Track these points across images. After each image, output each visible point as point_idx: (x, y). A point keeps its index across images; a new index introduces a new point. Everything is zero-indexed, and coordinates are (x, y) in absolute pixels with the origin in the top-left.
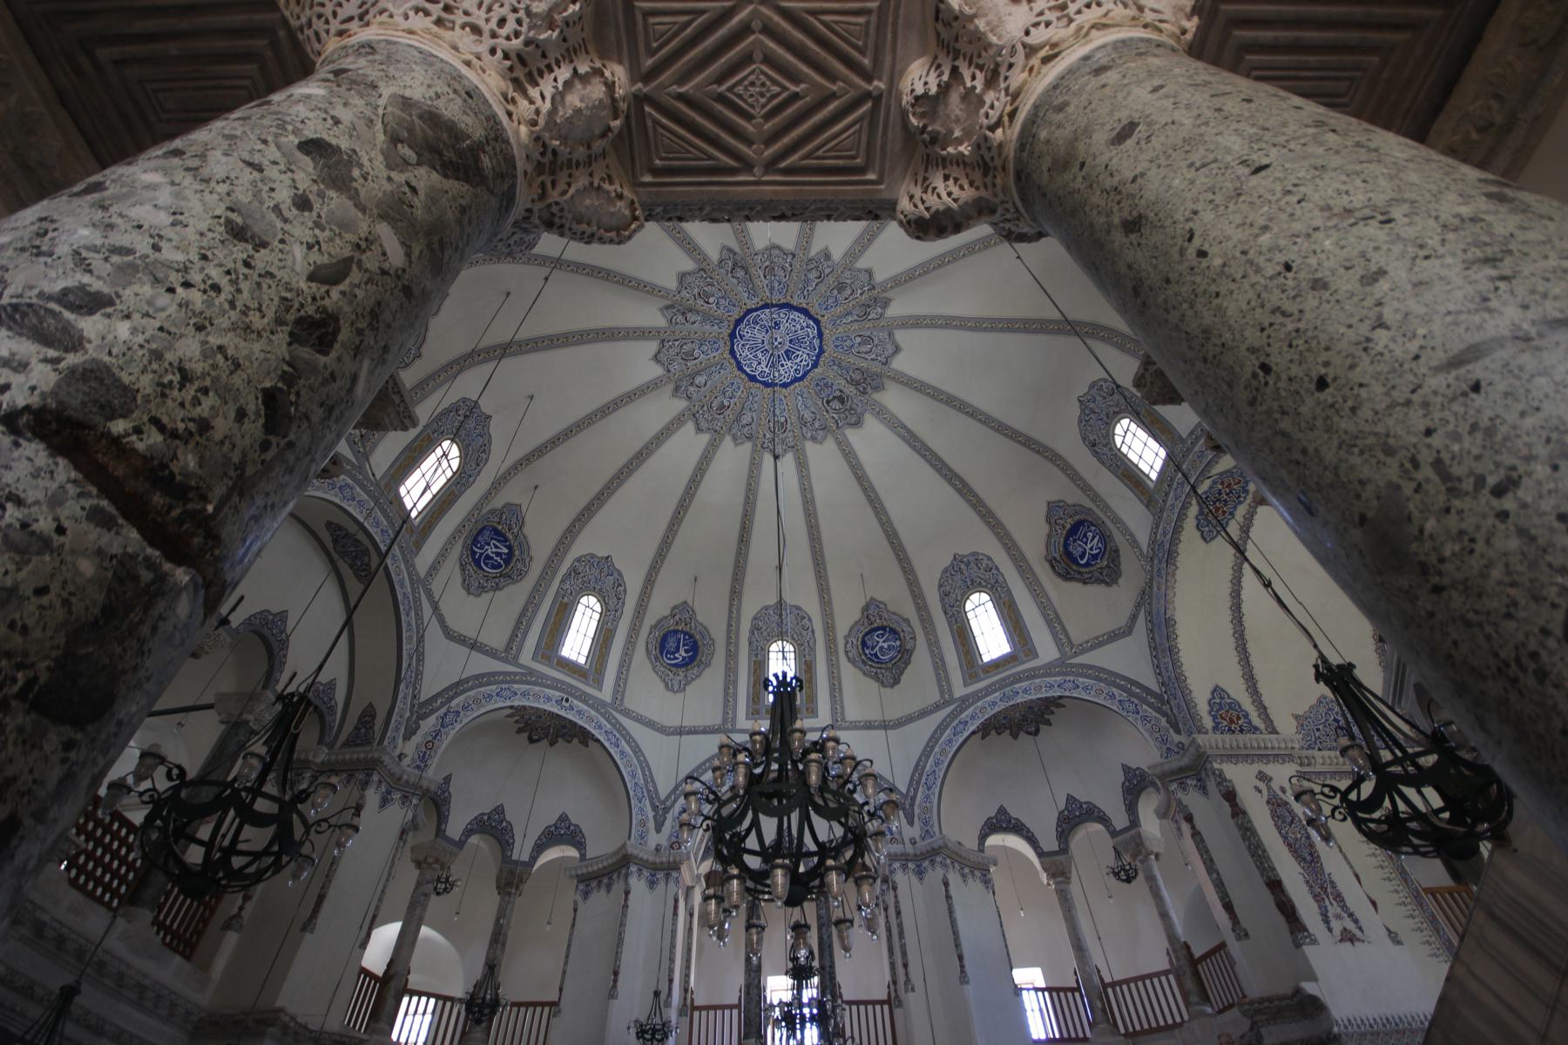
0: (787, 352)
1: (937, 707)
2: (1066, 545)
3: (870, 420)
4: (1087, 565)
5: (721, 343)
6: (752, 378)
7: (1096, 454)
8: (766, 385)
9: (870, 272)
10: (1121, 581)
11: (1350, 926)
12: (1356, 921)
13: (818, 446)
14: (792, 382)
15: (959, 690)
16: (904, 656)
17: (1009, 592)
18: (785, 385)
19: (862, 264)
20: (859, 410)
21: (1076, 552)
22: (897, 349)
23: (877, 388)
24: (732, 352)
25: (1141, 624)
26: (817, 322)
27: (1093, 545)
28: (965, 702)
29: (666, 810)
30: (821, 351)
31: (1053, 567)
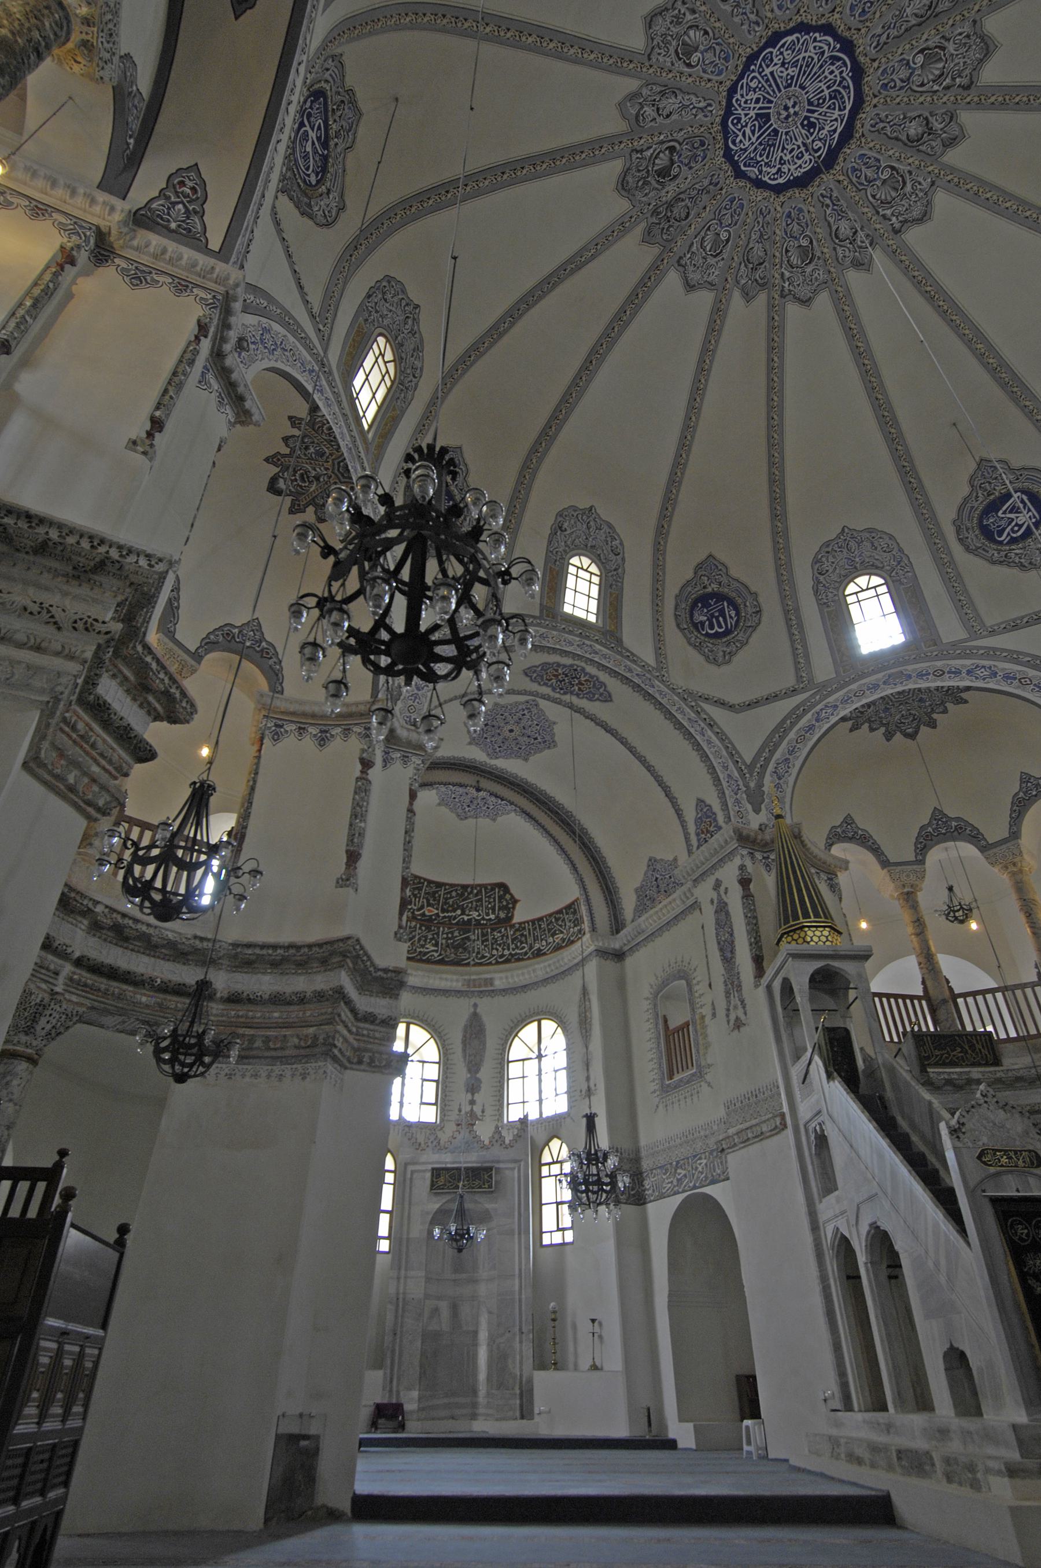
0: (767, 117)
3: (622, 205)
5: (854, 22)
6: (774, 39)
7: (553, 534)
8: (752, 58)
9: (806, 302)
13: (619, 97)
14: (729, 104)
18: (732, 91)
19: (823, 300)
20: (639, 195)
22: (690, 287)
23: (648, 238)
24: (828, 29)
26: (778, 190)
30: (739, 174)
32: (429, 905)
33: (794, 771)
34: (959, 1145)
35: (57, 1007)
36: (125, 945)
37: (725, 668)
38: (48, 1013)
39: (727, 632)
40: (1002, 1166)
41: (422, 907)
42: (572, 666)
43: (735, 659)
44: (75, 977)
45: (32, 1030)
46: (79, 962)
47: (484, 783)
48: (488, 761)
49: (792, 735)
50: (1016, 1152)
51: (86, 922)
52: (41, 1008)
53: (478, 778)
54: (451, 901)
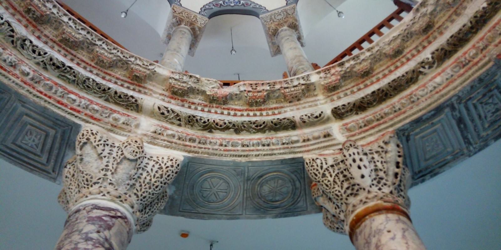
35: (352, 150)
36: (374, 79)
38: (350, 161)
44: (349, 125)
45: (356, 188)
46: (338, 114)
51: (321, 97)
52: (342, 165)
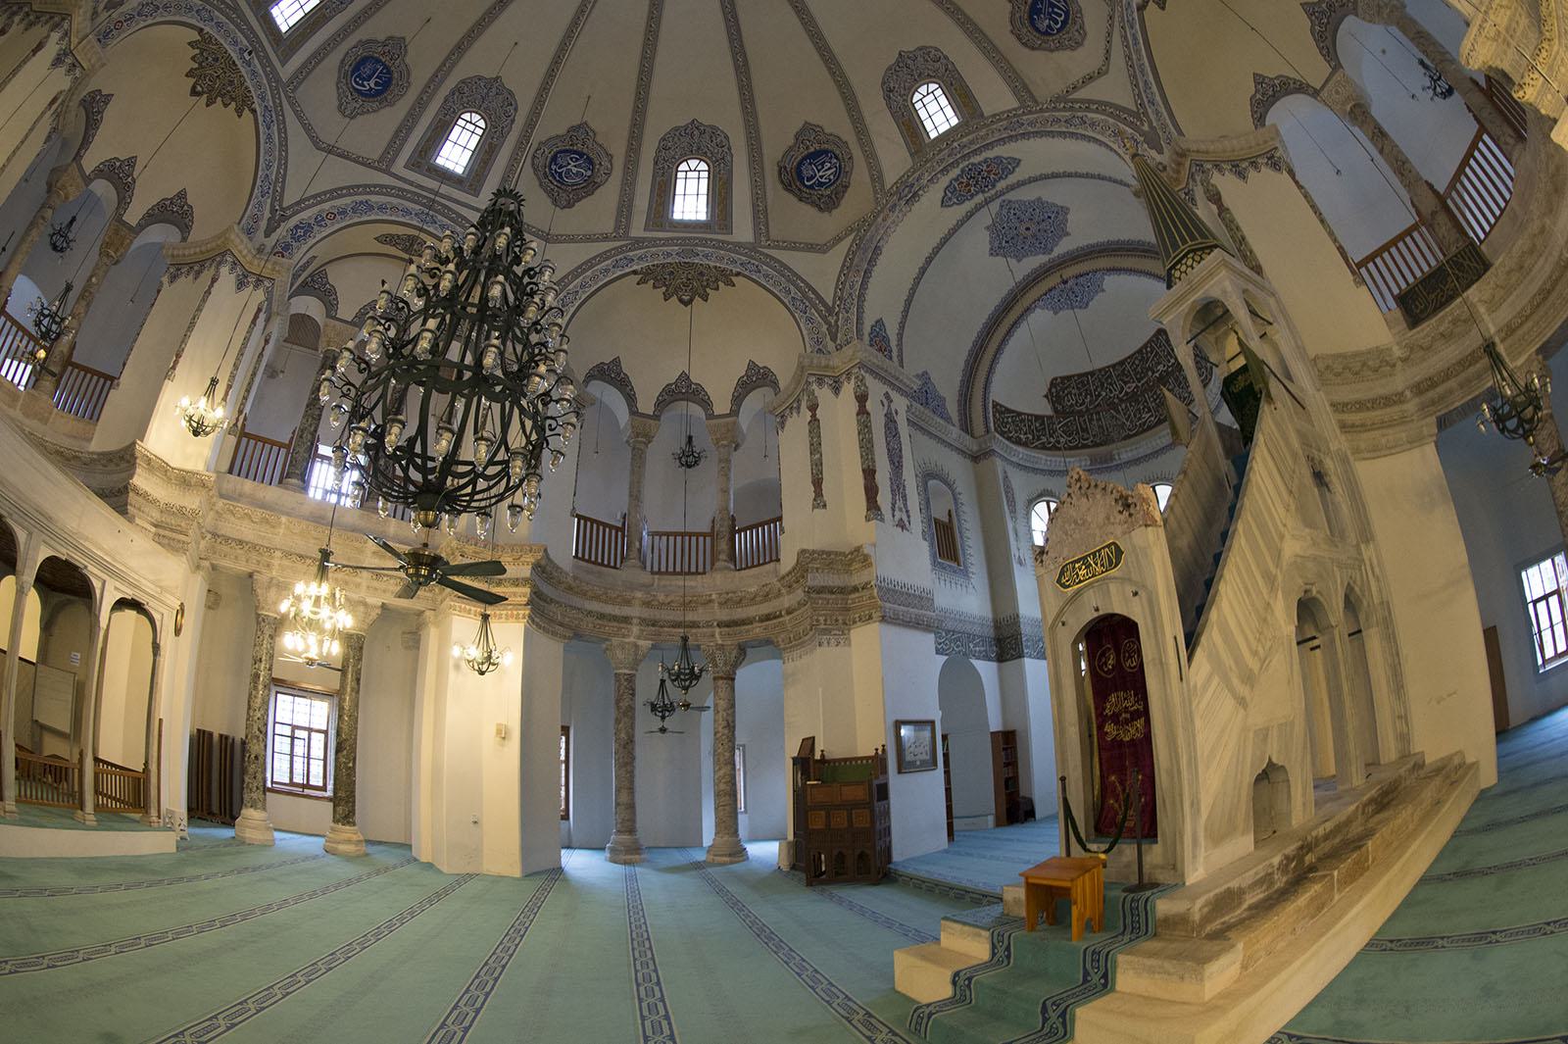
1: (606, 238)
2: (801, 163)
4: (811, 187)
10: (834, 212)
11: (905, 518)
12: (909, 517)
15: (637, 230)
16: (590, 186)
17: (731, 172)
21: (807, 171)
25: (843, 247)
27: (826, 173)
28: (638, 242)
29: (284, 218)
31: (780, 174)
32: (1126, 383)
33: (1154, 88)
34: (1042, 571)
37: (1086, 42)
39: (1067, 13)
40: (1080, 582)
41: (1122, 388)
42: (963, 171)
43: (1087, 27)
47: (1069, 272)
48: (1052, 256)
49: (1134, 57)
50: (1094, 554)
53: (1058, 274)
54: (1139, 369)
